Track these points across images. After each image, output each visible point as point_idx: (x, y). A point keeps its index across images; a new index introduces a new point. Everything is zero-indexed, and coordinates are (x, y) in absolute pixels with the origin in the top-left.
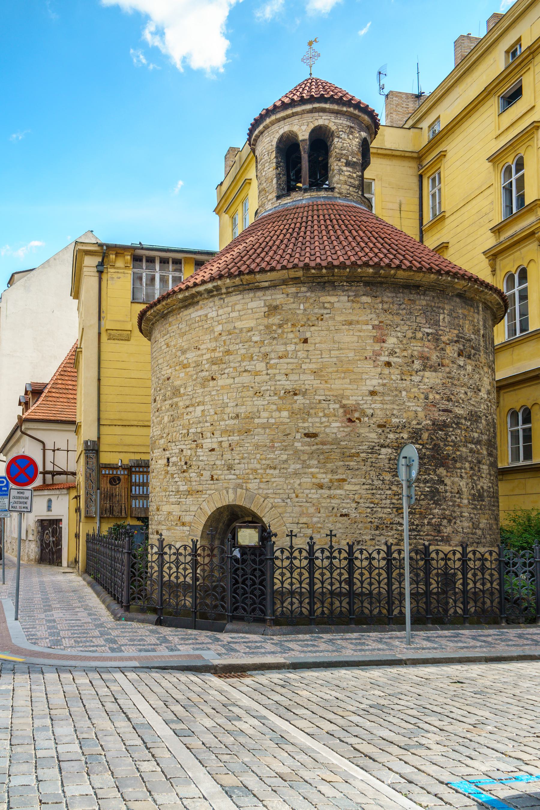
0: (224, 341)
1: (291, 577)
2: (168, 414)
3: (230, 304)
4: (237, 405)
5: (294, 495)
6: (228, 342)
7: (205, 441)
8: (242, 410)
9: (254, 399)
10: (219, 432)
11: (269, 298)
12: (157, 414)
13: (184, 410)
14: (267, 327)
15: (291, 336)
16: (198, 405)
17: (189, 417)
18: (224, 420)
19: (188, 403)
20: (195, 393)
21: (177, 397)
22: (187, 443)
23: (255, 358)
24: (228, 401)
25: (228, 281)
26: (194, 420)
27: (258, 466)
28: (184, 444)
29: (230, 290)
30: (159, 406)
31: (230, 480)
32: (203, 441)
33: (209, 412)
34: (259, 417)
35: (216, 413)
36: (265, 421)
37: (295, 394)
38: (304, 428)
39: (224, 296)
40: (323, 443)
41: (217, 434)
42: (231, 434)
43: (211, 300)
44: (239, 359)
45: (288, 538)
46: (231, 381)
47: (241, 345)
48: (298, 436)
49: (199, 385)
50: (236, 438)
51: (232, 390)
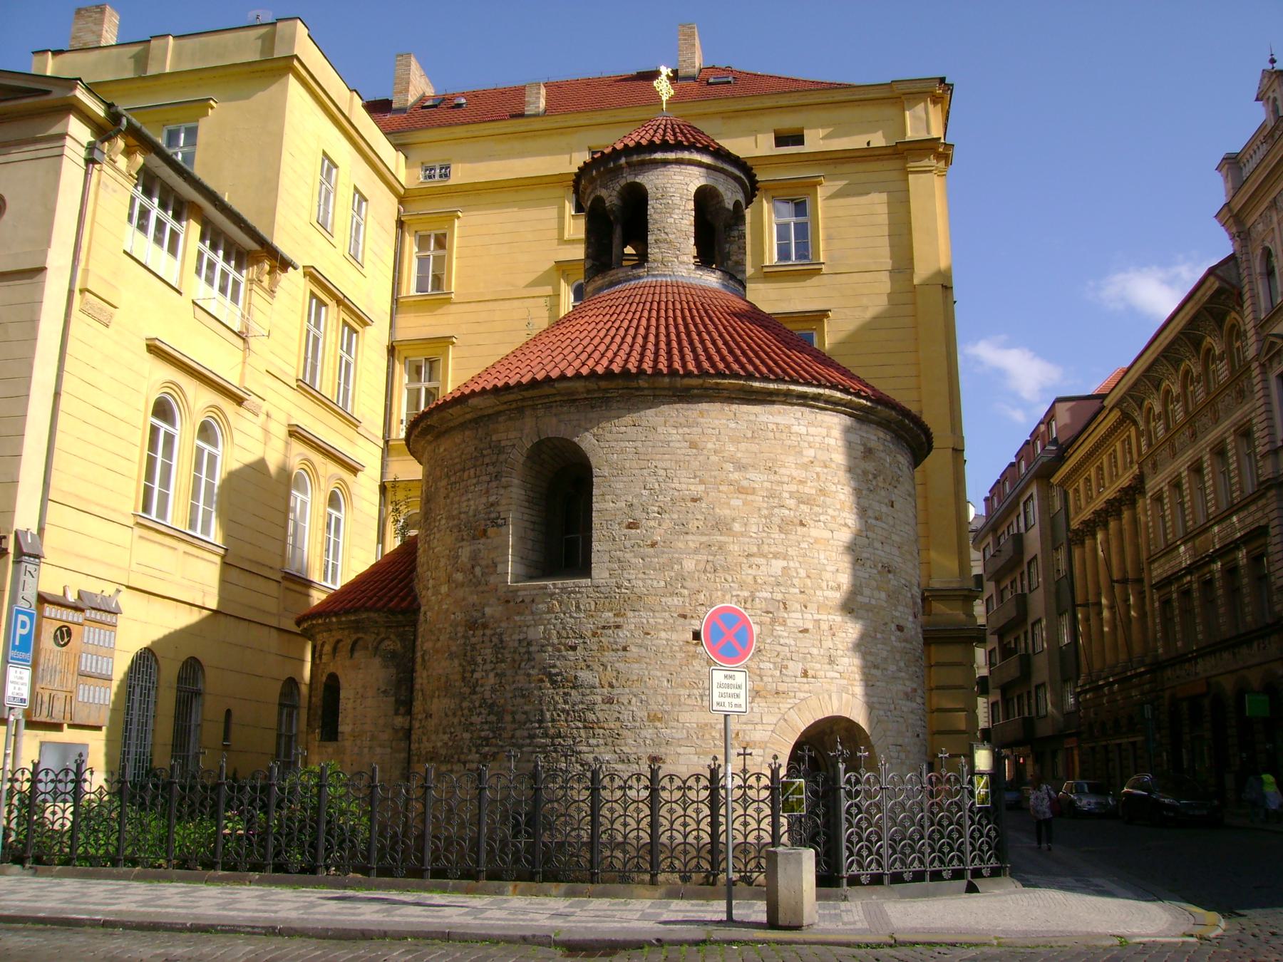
6: (823, 477)
7: (793, 615)
10: (815, 606)
11: (864, 435)
12: (651, 550)
13: (745, 561)
14: (865, 473)
15: (883, 493)
16: (776, 556)
18: (821, 589)
19: (755, 549)
24: (826, 562)
25: (839, 395)
26: (766, 579)
31: (832, 678)
32: (786, 615)
33: (797, 573)
34: (862, 594)
35: (808, 577)
36: (867, 600)
37: (889, 571)
38: (897, 617)
40: (906, 641)
41: (812, 607)
44: (838, 507)
46: (827, 534)
47: (839, 487)
48: (893, 627)
51: (830, 548)
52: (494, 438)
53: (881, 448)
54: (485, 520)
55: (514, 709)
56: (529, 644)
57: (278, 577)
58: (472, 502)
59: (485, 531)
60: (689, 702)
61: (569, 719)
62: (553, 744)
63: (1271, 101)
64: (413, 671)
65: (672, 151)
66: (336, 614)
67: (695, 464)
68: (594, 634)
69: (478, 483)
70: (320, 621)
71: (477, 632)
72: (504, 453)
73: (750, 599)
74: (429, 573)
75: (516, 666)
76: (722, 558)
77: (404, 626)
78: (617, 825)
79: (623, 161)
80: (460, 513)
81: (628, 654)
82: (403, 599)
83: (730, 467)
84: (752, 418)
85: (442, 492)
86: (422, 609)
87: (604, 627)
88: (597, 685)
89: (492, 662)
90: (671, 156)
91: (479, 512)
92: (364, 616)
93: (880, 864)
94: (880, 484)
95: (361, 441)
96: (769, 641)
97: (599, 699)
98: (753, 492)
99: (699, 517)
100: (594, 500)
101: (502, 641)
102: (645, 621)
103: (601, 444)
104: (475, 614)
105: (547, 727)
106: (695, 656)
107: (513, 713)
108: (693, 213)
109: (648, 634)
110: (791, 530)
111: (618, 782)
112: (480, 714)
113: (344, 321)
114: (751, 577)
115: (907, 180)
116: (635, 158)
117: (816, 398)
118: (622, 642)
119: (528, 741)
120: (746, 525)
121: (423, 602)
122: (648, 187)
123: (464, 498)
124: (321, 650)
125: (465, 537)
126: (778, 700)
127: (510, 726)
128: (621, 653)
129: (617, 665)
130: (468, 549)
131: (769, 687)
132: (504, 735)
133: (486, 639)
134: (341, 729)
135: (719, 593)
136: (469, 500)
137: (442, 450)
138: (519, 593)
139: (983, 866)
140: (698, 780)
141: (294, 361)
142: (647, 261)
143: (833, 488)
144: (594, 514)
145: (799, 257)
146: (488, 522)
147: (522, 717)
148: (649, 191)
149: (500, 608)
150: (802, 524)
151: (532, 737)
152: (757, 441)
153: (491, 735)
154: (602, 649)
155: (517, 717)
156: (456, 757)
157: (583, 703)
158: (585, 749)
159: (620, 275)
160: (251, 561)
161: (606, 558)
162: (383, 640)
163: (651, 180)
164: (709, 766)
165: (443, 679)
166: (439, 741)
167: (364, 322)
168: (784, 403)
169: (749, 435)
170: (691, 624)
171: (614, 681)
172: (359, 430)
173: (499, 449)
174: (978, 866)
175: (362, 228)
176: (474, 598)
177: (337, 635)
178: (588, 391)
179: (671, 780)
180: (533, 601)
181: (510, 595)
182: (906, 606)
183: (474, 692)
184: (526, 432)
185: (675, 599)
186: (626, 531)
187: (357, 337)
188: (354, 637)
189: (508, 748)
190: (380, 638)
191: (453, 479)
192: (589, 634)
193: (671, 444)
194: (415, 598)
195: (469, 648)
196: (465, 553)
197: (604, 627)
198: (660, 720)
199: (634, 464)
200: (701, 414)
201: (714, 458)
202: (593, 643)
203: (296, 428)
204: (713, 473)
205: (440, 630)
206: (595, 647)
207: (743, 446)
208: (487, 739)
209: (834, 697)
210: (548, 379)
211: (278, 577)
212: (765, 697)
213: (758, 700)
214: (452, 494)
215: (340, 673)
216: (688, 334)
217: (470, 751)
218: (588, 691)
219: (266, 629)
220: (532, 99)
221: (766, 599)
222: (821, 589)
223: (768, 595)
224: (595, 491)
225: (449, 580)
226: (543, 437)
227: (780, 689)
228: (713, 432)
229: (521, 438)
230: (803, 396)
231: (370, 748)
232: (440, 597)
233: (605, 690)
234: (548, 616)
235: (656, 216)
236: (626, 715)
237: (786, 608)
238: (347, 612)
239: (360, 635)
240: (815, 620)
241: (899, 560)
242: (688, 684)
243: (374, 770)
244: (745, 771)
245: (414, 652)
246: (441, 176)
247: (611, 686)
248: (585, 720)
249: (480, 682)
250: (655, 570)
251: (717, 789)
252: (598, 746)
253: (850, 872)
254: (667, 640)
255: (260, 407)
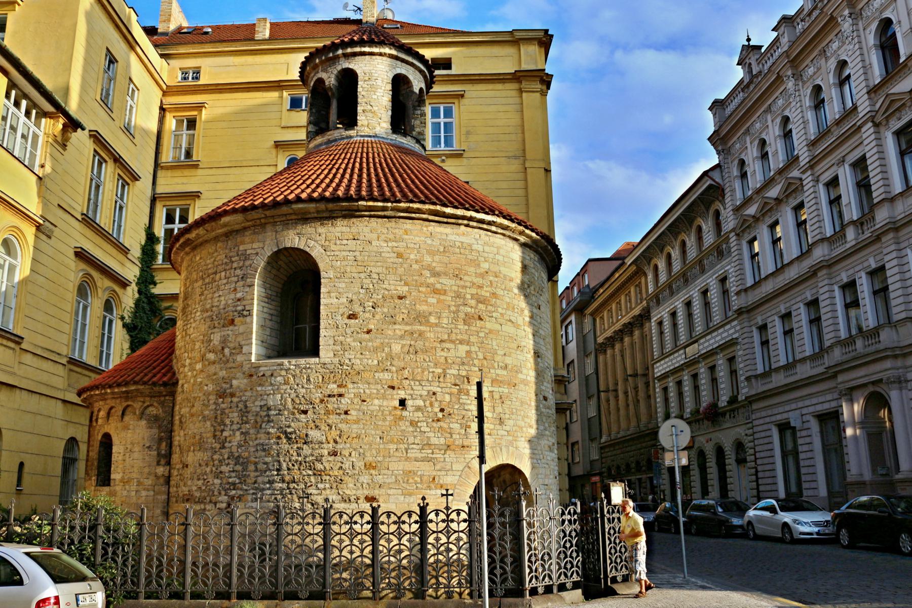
0: (491, 282)
1: (352, 545)
2: (401, 342)
3: (495, 245)
4: (505, 354)
5: (541, 456)
6: (494, 285)
8: (508, 360)
9: (518, 352)
12: (367, 336)
15: (534, 299)
16: (461, 343)
17: (445, 354)
18: (494, 368)
19: (446, 337)
20: (456, 328)
21: (421, 324)
22: (442, 385)
23: (516, 310)
24: (497, 348)
27: (523, 424)
28: (439, 386)
29: (500, 231)
30: (372, 327)
32: (469, 388)
33: (477, 356)
34: (521, 373)
35: (485, 358)
36: (524, 377)
39: (489, 233)
42: (501, 385)
43: (476, 230)
44: (505, 307)
45: (444, 499)
46: (498, 327)
47: (506, 292)
49: (461, 322)
50: (506, 391)
52: (241, 248)
53: (532, 266)
54: (233, 311)
55: (257, 460)
56: (269, 409)
57: (64, 361)
58: (222, 298)
59: (233, 321)
60: (397, 454)
61: (302, 468)
62: (289, 488)
63: (747, 65)
64: (171, 431)
65: (376, 47)
66: (110, 387)
67: (401, 271)
68: (322, 401)
69: (227, 283)
70: (97, 392)
71: (226, 400)
72: (249, 259)
73: (443, 375)
74: (186, 355)
75: (258, 426)
76: (422, 343)
77: (165, 396)
78: (344, 553)
79: (340, 52)
80: (213, 307)
81: (349, 417)
82: (164, 375)
83: (427, 274)
84: (444, 237)
85: (198, 291)
86: (180, 382)
87: (329, 396)
88: (324, 441)
89: (238, 423)
90: (376, 50)
91: (229, 306)
92: (133, 388)
93: (550, 578)
94: (533, 292)
95: (129, 264)
96: (456, 407)
97: (326, 452)
98: (445, 293)
99: (404, 311)
100: (322, 296)
101: (246, 407)
102: (362, 392)
103: (328, 253)
104: (224, 386)
105: (283, 474)
106: (401, 418)
107: (256, 463)
108: (391, 93)
109: (364, 401)
110: (473, 323)
111: (345, 517)
112: (228, 464)
113: (119, 175)
114: (443, 358)
115: (521, 97)
116: (349, 50)
117: (490, 223)
118: (344, 407)
119: (268, 486)
120: (439, 318)
121: (181, 377)
122: (358, 72)
123: (217, 295)
124: (98, 415)
125: (216, 325)
126: (463, 452)
127: (253, 474)
128: (343, 416)
129: (340, 425)
130: (219, 334)
131: (457, 443)
132: (249, 481)
133: (233, 405)
134: (112, 476)
135: (419, 370)
136: (220, 296)
137: (198, 258)
138: (261, 369)
139: (617, 574)
140: (410, 516)
141: (80, 200)
142: (357, 125)
143: (501, 293)
144: (322, 307)
145: (446, 144)
146: (235, 313)
147: (261, 466)
148: (359, 75)
149: (245, 381)
150: (480, 319)
151: (271, 482)
152: (447, 255)
153: (237, 481)
154: (328, 413)
155: (259, 466)
156: (208, 499)
157: (313, 455)
158: (315, 492)
159: (335, 135)
160: (42, 348)
161: (331, 342)
162: (148, 406)
163: (359, 65)
164: (419, 505)
165: (198, 437)
166: (193, 486)
167: (135, 178)
168: (467, 226)
169: (442, 249)
170: (398, 394)
171: (338, 438)
172: (129, 256)
173: (246, 257)
174: (614, 575)
175: (134, 110)
176: (223, 373)
177: (111, 403)
178: (318, 212)
179: (389, 517)
180: (272, 375)
181: (254, 370)
182: (548, 382)
183: (223, 447)
184: (267, 243)
185: (386, 374)
186: (347, 321)
187: (128, 189)
188: (125, 404)
189: (252, 491)
190: (146, 405)
191: (207, 281)
192: (318, 401)
193: (383, 255)
194: (174, 374)
195: (219, 412)
196: (216, 339)
197: (329, 396)
198: (374, 468)
199: (354, 270)
200: (406, 232)
201: (415, 266)
202: (321, 409)
203: (79, 250)
204: (414, 278)
205: (195, 398)
206: (322, 412)
207: (437, 258)
208: (234, 484)
209: (504, 449)
210: (286, 202)
211: (64, 361)
212: (454, 450)
213: (448, 452)
214: (206, 292)
215: (112, 433)
216: (393, 175)
217: (220, 493)
218: (317, 446)
219: (54, 400)
220: (260, 30)
221: (454, 375)
222: (494, 368)
223: (455, 372)
224: (323, 290)
225: (203, 358)
226: (281, 247)
227: (465, 444)
228: (415, 246)
229: (263, 248)
230: (482, 221)
231: (136, 491)
232: (195, 373)
233: (330, 445)
234: (284, 387)
235: (363, 93)
236: (347, 465)
237: (469, 382)
238: (119, 385)
239: (129, 403)
240: (490, 392)
241: (544, 348)
242: (396, 440)
243: (142, 510)
244: (447, 508)
245: (172, 416)
246: (193, 78)
247: (336, 442)
248: (314, 469)
249: (228, 440)
250: (370, 351)
251: (426, 522)
252: (325, 489)
253: (531, 586)
254: (380, 406)
255: (53, 232)
